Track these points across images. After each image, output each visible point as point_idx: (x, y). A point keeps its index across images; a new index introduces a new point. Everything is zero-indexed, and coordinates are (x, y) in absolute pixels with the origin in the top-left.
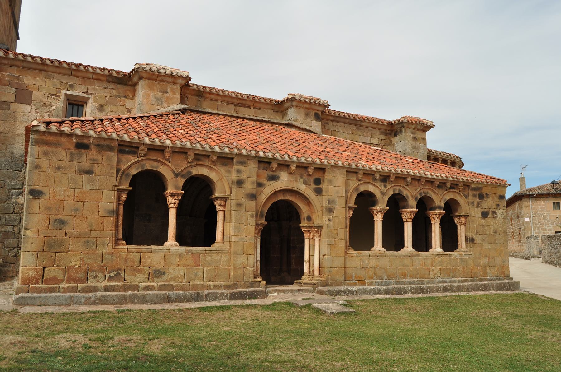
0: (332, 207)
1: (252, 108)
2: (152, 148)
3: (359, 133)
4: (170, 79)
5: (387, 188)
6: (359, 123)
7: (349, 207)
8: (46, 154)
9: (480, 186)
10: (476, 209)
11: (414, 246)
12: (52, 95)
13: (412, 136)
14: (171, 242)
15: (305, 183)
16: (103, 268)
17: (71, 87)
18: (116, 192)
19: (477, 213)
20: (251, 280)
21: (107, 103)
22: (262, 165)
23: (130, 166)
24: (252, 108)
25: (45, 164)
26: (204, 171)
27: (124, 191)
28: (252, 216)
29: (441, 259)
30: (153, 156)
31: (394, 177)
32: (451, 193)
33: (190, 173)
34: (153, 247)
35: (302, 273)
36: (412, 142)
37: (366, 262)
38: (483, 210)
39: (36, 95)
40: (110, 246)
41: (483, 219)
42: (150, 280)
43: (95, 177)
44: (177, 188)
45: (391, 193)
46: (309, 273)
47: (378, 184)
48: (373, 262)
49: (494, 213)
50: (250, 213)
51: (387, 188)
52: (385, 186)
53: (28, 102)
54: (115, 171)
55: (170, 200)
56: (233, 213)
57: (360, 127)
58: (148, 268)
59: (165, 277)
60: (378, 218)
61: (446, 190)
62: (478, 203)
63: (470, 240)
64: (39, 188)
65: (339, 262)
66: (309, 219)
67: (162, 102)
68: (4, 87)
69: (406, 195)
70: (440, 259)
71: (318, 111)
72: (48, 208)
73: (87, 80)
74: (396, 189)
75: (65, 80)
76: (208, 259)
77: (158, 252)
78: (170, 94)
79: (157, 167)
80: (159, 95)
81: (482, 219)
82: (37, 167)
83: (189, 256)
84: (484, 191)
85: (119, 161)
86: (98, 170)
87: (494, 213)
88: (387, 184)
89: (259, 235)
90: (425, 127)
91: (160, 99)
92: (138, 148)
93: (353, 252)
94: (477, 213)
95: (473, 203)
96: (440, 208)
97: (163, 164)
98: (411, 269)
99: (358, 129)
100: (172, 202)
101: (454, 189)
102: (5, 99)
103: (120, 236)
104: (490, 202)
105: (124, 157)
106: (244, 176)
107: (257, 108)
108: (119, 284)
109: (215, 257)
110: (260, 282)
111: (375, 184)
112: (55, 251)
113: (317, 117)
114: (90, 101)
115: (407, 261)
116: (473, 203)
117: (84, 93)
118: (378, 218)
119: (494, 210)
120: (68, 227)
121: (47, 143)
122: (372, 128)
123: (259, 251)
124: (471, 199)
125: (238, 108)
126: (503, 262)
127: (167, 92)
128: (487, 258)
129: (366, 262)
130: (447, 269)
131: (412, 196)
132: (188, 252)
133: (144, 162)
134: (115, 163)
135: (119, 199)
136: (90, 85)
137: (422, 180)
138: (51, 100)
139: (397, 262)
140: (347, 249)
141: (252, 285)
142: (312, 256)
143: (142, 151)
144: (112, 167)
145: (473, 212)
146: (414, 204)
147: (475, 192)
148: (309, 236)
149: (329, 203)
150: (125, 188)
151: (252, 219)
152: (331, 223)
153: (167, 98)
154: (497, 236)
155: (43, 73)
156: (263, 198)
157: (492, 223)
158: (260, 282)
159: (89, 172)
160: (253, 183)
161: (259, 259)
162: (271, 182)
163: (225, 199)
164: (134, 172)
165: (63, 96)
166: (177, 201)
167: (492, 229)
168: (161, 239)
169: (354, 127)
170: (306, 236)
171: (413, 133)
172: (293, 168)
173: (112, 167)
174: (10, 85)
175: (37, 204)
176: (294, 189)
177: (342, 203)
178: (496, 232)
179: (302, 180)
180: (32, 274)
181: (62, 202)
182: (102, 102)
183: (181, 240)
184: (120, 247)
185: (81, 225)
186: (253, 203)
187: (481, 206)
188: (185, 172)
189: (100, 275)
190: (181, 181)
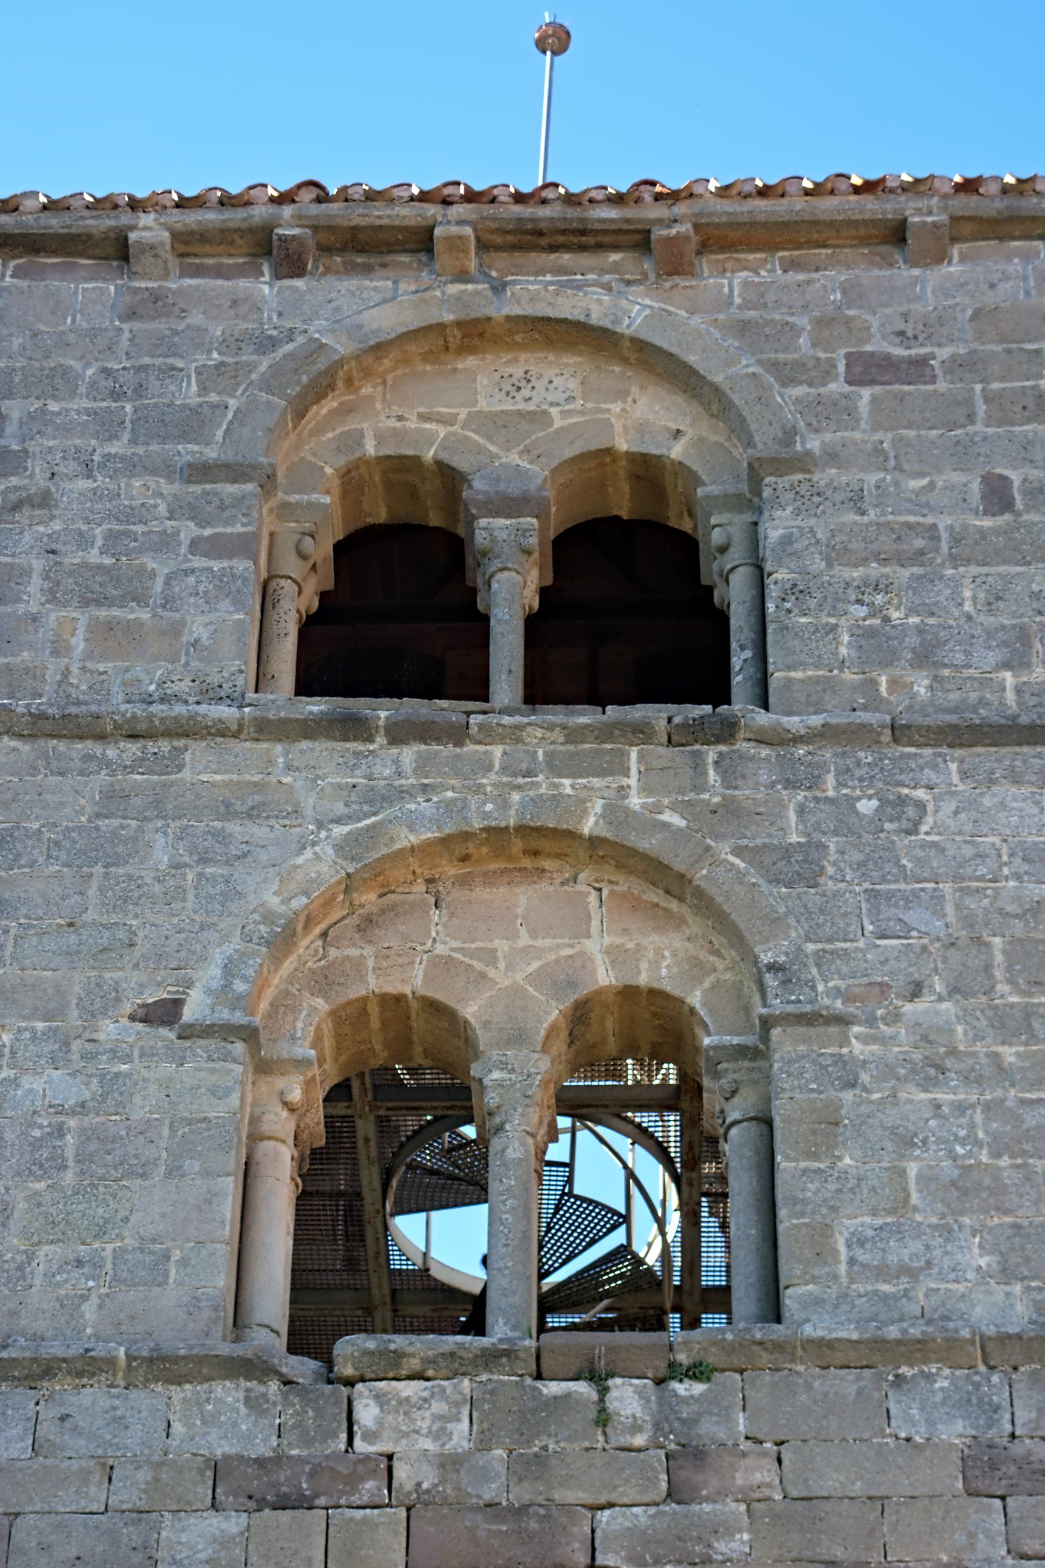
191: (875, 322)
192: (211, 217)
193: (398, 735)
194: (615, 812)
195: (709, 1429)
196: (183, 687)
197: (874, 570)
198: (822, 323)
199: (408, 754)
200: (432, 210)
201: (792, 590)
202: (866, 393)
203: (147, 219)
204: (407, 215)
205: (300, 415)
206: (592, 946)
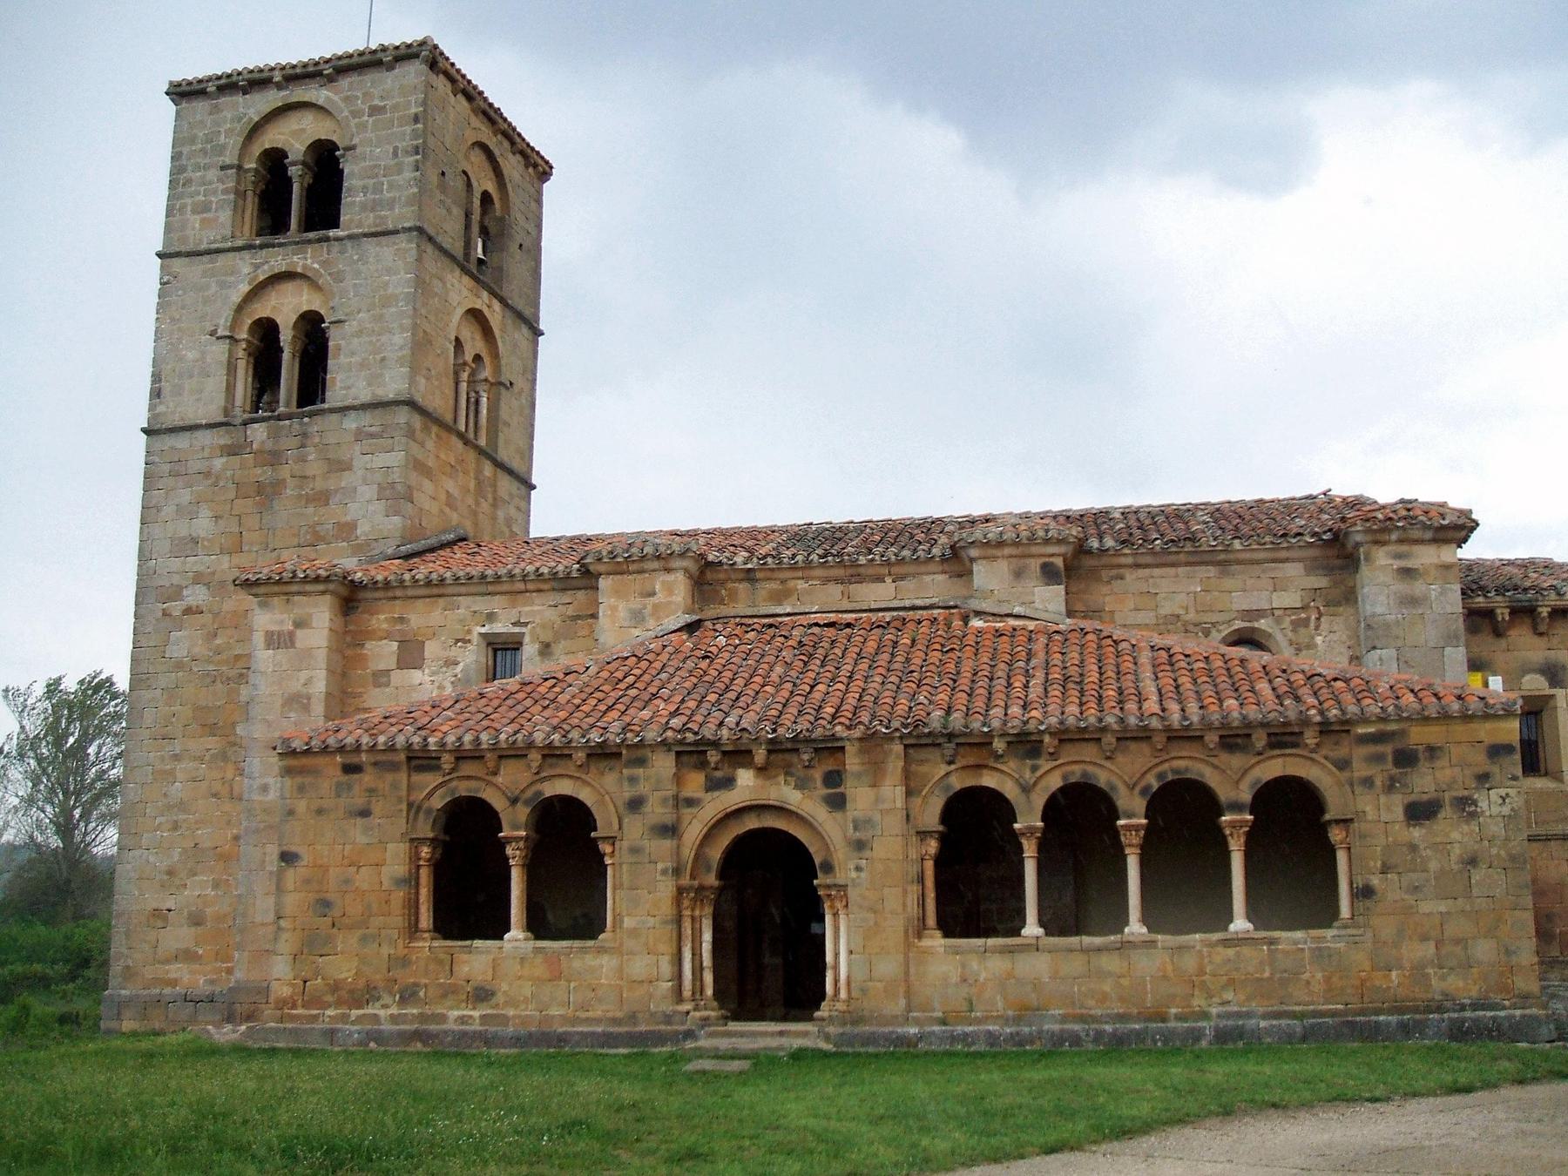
0: (864, 838)
1: (888, 580)
2: (461, 756)
3: (1228, 583)
4: (655, 565)
5: (1038, 774)
6: (1222, 557)
7: (917, 833)
8: (301, 789)
9: (1392, 727)
10: (1383, 799)
11: (1145, 920)
12: (458, 641)
13: (1397, 564)
14: (516, 933)
15: (800, 786)
17: (491, 617)
18: (408, 844)
19: (1389, 809)
20: (668, 1007)
21: (558, 636)
22: (685, 758)
23: (430, 794)
24: (888, 580)
25: (301, 806)
26: (564, 787)
27: (422, 841)
28: (664, 872)
29: (1238, 954)
30: (468, 768)
31: (1056, 742)
32: (1280, 760)
33: (539, 793)
34: (478, 943)
35: (823, 996)
36: (1402, 587)
37: (975, 965)
38: (1413, 798)
39: (431, 649)
40: (400, 942)
41: (1415, 826)
42: (470, 1006)
43: (375, 820)
44: (516, 827)
45: (1055, 782)
46: (835, 996)
47: (1011, 765)
49: (1464, 804)
50: (660, 866)
51: (1038, 774)
52: (1034, 769)
53: (418, 666)
54: (404, 806)
55: (509, 851)
57: (1232, 568)
58: (464, 983)
60: (1030, 850)
61: (1260, 754)
62: (1392, 779)
63: (1364, 893)
64: (293, 849)
65: (888, 967)
66: (828, 867)
67: (643, 619)
68: (380, 643)
69: (1109, 783)
70: (1231, 952)
71: (1052, 555)
72: (307, 881)
73: (519, 595)
74: (1073, 773)
75: (482, 605)
76: (577, 964)
77: (483, 953)
78: (660, 597)
79: (478, 790)
80: (636, 603)
81: (1409, 825)
83: (539, 959)
84: (1419, 736)
85: (410, 788)
86: (377, 808)
87: (1465, 805)
88: (1040, 762)
89: (709, 910)
90: (1460, 527)
91: (640, 612)
92: (439, 758)
93: (936, 941)
94: (1389, 809)
95: (1368, 782)
96: (1236, 807)
97: (489, 783)
98: (1125, 982)
99: (1224, 574)
100: (515, 855)
101: (1295, 745)
102: (382, 666)
103: (426, 920)
104: (1448, 772)
105: (417, 778)
106: (643, 788)
107: (903, 578)
108: (415, 1011)
109: (591, 960)
110: (688, 1013)
111: (999, 766)
112: (320, 953)
113: (1050, 574)
114: (527, 639)
115: (1110, 963)
116: (1368, 782)
117: (514, 624)
118: (1030, 850)
119: (1466, 793)
120: (336, 912)
121: (302, 771)
122: (1274, 561)
124: (1360, 770)
125: (851, 587)
126: (1508, 952)
127: (653, 594)
128: (1432, 944)
129: (975, 965)
130: (1259, 980)
131: (1132, 788)
132: (537, 950)
133: (454, 783)
134: (404, 793)
135: (415, 857)
136: (525, 605)
137: (1155, 739)
138: (455, 652)
139: (1076, 965)
141: (668, 1019)
142: (837, 955)
143: (447, 760)
144: (400, 800)
145: (1368, 809)
146: (1140, 804)
147: (1379, 748)
148: (832, 907)
149: (856, 828)
150: (422, 836)
151: (664, 878)
152: (863, 875)
153: (656, 607)
154: (1477, 876)
155: (441, 601)
156: (694, 831)
157: (1455, 835)
158: (688, 1013)
159: (365, 813)
160: (665, 800)
161: (707, 960)
162: (716, 794)
163: (612, 840)
164: (438, 802)
165: (475, 638)
166: (518, 852)
167: (1457, 851)
169: (1212, 571)
170: (826, 905)
171: (1399, 556)
172: (760, 755)
174: (388, 636)
176: (771, 802)
177: (895, 824)
178: (1472, 861)
179: (792, 780)
181: (325, 869)
182: (547, 636)
183: (538, 927)
184: (416, 945)
185: (355, 909)
186: (667, 844)
187: (1405, 785)
188: (529, 794)
190: (523, 812)
191: (376, 92)
192: (223, 81)
198: (365, 95)
199: (264, 251)
202: (371, 120)
203: (210, 84)
204: (266, 75)
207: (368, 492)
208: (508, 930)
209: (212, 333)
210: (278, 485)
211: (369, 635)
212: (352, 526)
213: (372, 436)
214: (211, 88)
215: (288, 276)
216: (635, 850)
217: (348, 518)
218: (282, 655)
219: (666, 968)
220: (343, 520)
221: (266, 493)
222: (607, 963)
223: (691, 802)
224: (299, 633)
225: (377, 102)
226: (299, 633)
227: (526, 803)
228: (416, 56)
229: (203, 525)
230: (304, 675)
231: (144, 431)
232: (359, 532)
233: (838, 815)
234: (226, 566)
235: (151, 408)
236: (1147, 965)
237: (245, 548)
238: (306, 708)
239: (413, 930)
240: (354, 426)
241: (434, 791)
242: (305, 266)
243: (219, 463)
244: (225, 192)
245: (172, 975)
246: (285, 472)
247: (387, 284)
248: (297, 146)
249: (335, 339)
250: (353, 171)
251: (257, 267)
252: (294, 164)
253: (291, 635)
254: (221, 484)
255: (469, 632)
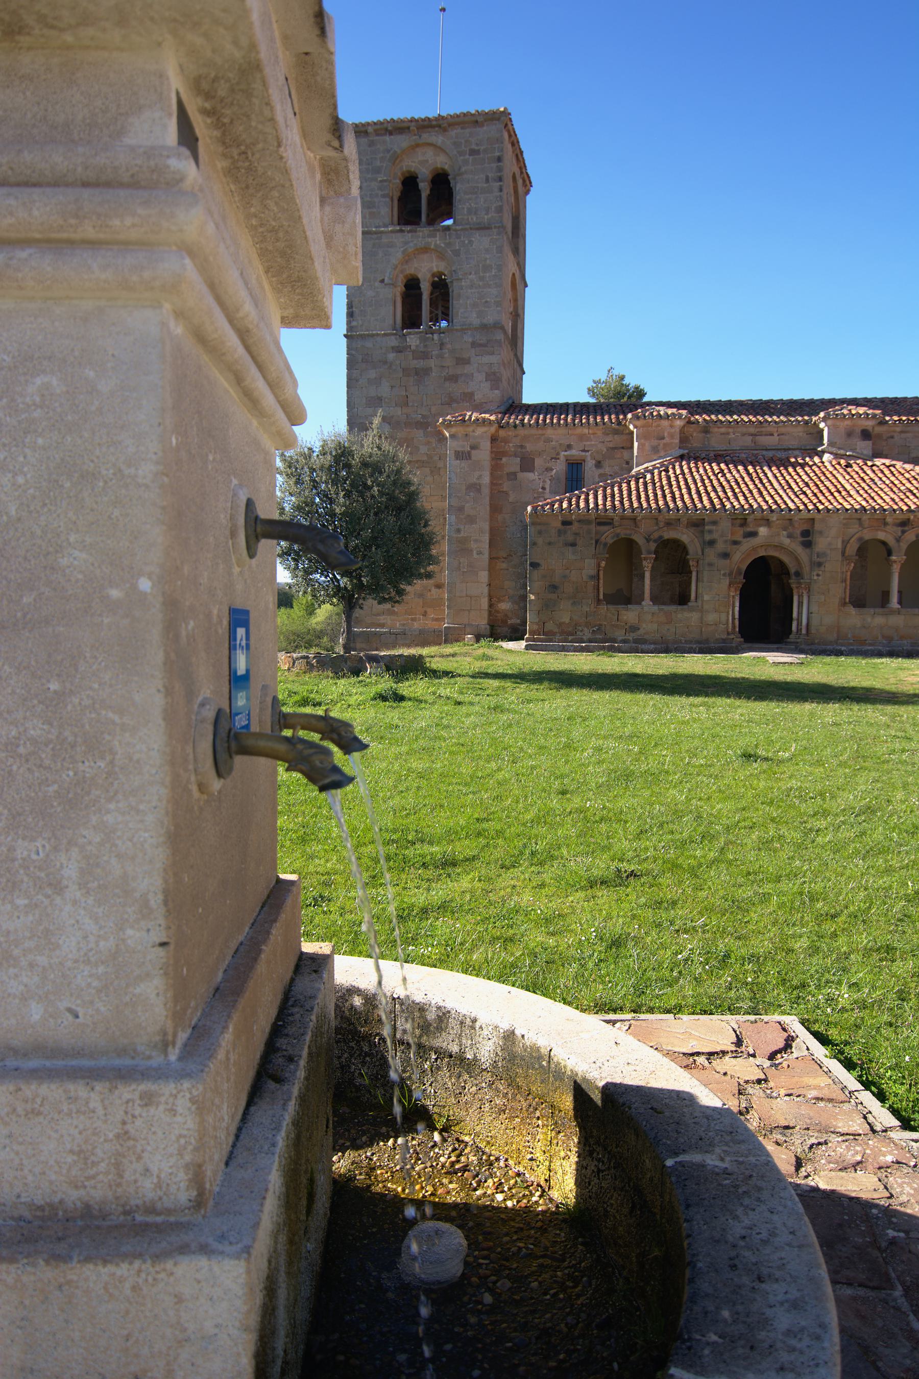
14: (647, 602)
16: (588, 625)
25: (540, 541)
28: (724, 575)
33: (661, 537)
34: (629, 606)
39: (538, 462)
48: (879, 620)
50: (722, 572)
55: (645, 563)
56: (705, 573)
59: (639, 632)
64: (537, 561)
82: (534, 544)
93: (852, 610)
102: (512, 470)
109: (686, 614)
114: (589, 458)
123: (737, 609)
127: (663, 438)
129: (869, 620)
135: (599, 565)
138: (551, 464)
140: (844, 604)
142: (800, 613)
144: (591, 538)
148: (798, 592)
152: (820, 578)
153: (665, 445)
156: (737, 557)
159: (573, 545)
161: (737, 616)
168: (639, 601)
170: (795, 592)
173: (591, 538)
174: (516, 456)
175: (536, 574)
180: (535, 627)
182: (599, 458)
183: (655, 599)
189: (586, 629)
190: (653, 546)
193: (409, 232)
194: (436, 245)
195: (444, 341)
196: (381, 224)
197: (470, 196)
200: (410, 124)
201: (460, 201)
204: (405, 125)
205: (394, 164)
206: (434, 265)
207: (480, 377)
208: (643, 600)
209: (382, 281)
210: (427, 371)
211: (505, 454)
212: (472, 394)
213: (481, 345)
214: (370, 129)
215: (425, 250)
216: (710, 565)
217: (470, 390)
218: (464, 464)
219: (724, 616)
220: (466, 391)
221: (421, 374)
222: (695, 616)
223: (735, 543)
224: (473, 452)
225: (474, 147)
226: (473, 452)
227: (655, 541)
228: (499, 119)
229: (384, 390)
230: (477, 474)
231: (345, 336)
232: (476, 397)
233: (808, 550)
234: (400, 413)
235: (348, 323)
236: (897, 621)
237: (410, 404)
238: (479, 491)
239: (599, 601)
240: (470, 340)
241: (608, 536)
242: (436, 245)
243: (391, 356)
244: (384, 196)
245: (382, 622)
246: (432, 363)
247: (486, 259)
248: (424, 170)
249: (454, 289)
250: (460, 188)
251: (406, 243)
252: (423, 181)
253: (469, 453)
254: (394, 367)
255: (558, 454)
